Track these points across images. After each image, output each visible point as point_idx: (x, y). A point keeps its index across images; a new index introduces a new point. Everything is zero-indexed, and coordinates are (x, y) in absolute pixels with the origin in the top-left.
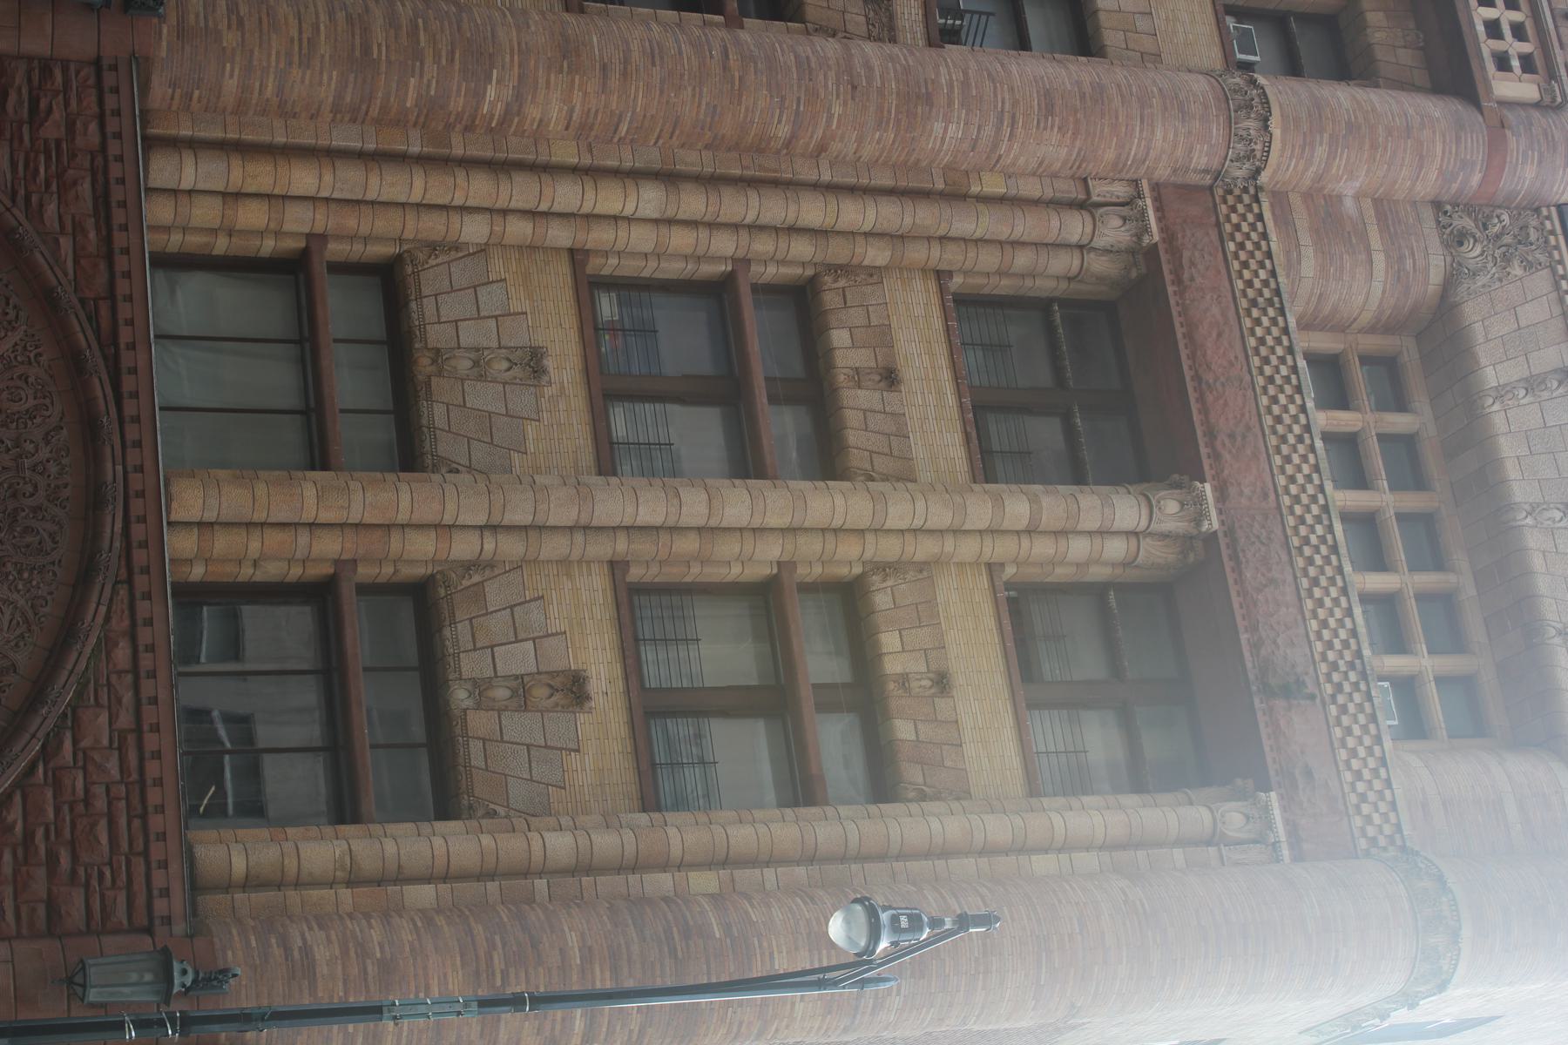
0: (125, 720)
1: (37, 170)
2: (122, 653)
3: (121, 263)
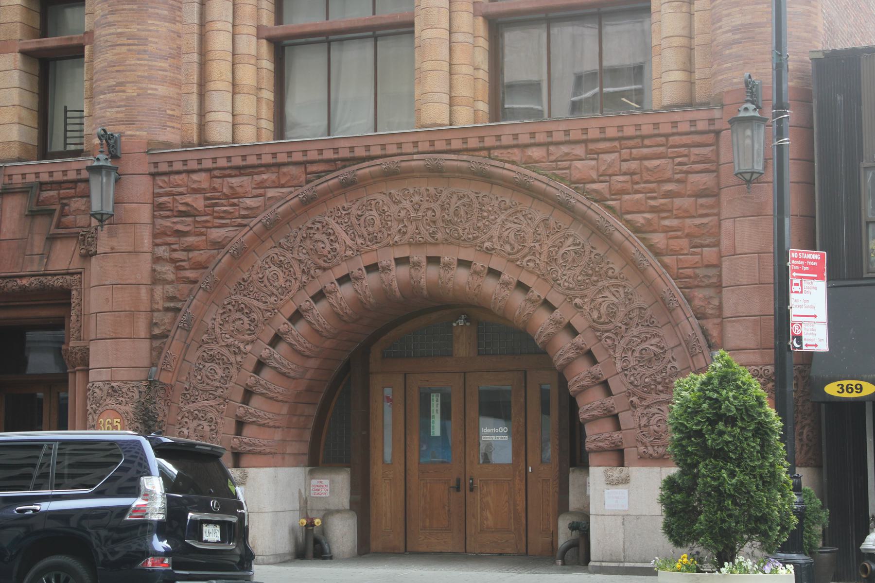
0: (579, 150)
1: (225, 211)
2: (536, 153)
3: (282, 158)
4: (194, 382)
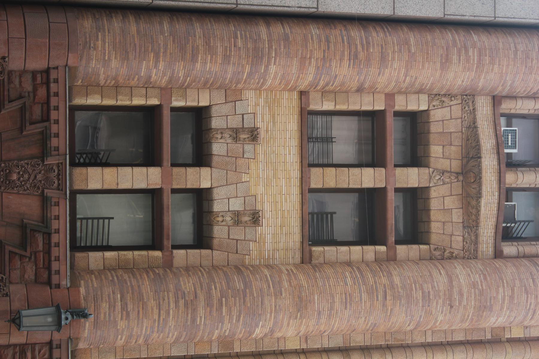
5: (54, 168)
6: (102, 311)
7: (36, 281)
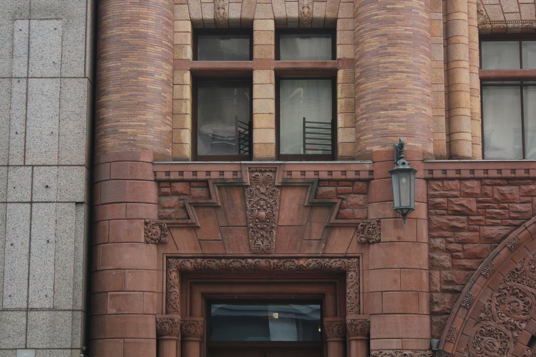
1: (497, 213)
4: (474, 352)
5: (254, 176)
6: (397, 129)
7: (366, 193)
